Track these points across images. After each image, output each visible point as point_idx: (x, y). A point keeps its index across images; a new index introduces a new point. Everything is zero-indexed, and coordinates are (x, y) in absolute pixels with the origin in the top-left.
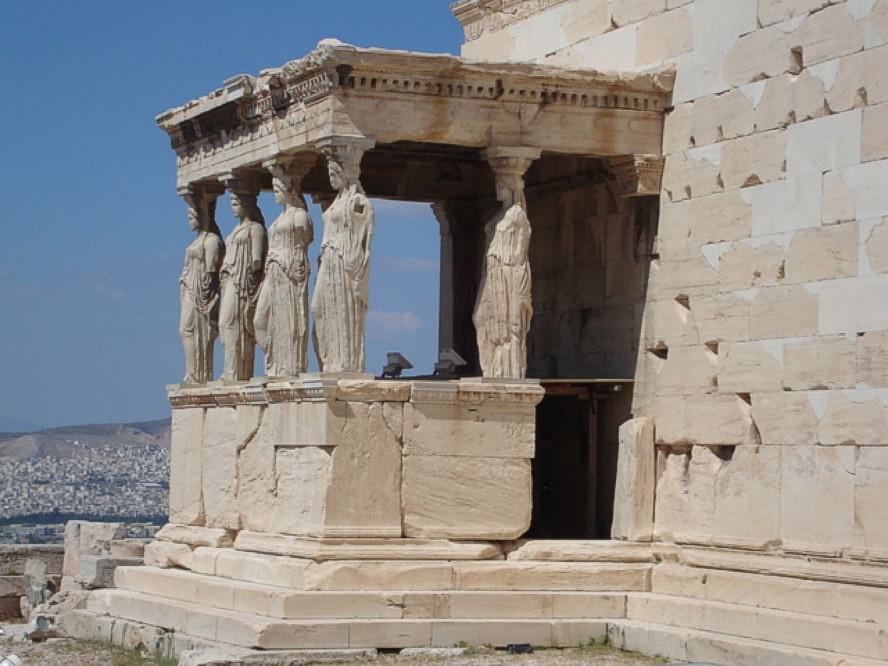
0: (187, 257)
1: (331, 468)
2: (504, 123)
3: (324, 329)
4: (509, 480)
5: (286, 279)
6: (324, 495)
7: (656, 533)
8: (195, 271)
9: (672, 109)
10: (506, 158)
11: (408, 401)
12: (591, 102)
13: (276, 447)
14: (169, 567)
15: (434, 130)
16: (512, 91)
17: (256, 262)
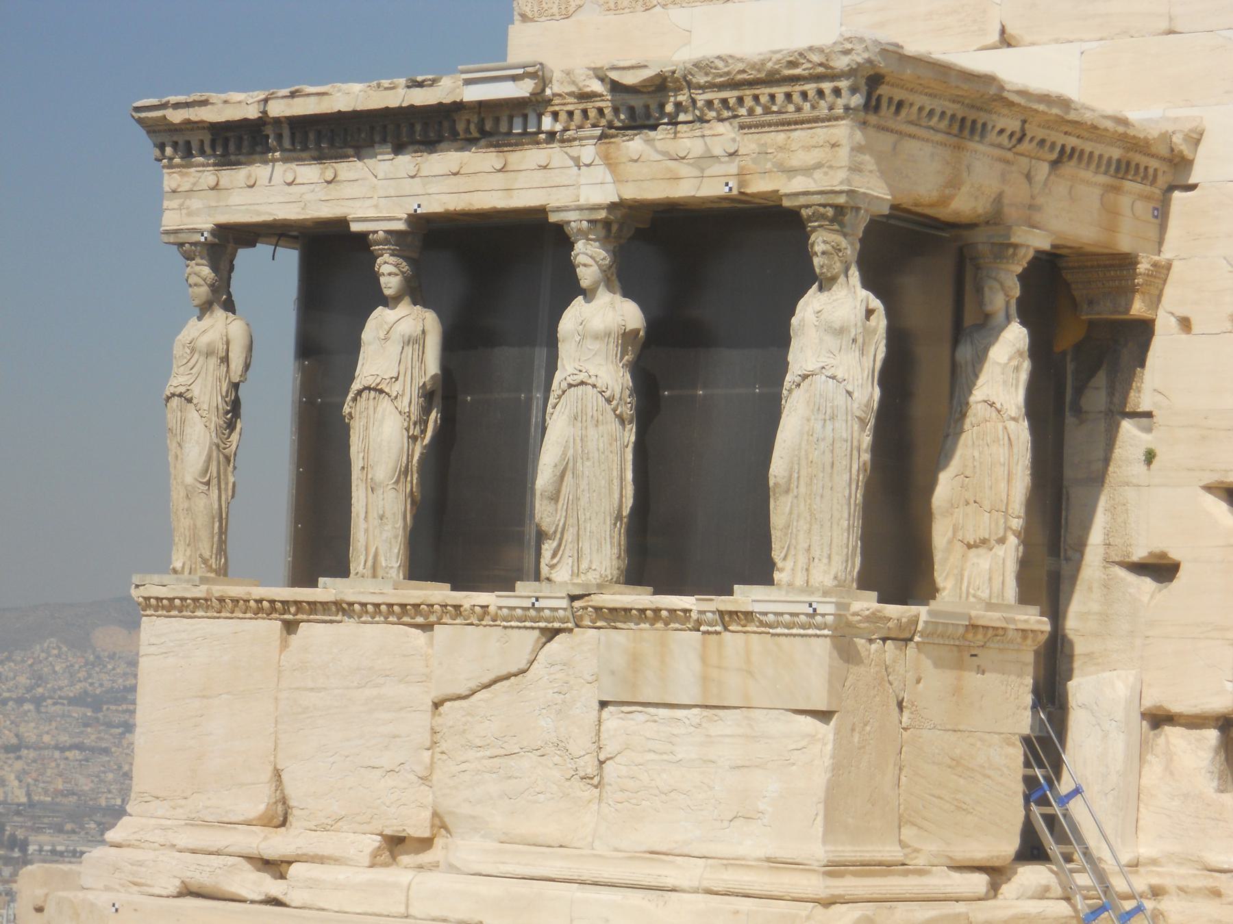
0: (178, 350)
1: (830, 747)
2: (1016, 192)
3: (791, 513)
4: (1005, 770)
5: (610, 416)
6: (821, 794)
7: (1145, 850)
8: (210, 379)
9: (1192, 187)
10: (1016, 246)
11: (911, 639)
12: (1103, 168)
13: (603, 704)
14: (180, 895)
15: (947, 191)
16: (1032, 139)
17: (434, 377)
